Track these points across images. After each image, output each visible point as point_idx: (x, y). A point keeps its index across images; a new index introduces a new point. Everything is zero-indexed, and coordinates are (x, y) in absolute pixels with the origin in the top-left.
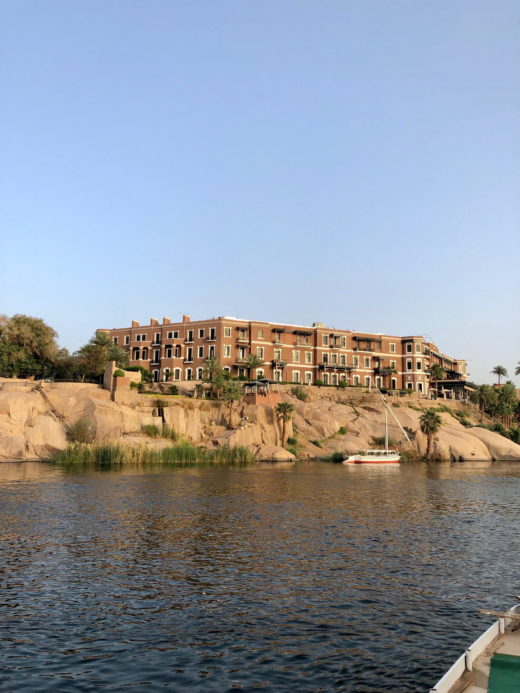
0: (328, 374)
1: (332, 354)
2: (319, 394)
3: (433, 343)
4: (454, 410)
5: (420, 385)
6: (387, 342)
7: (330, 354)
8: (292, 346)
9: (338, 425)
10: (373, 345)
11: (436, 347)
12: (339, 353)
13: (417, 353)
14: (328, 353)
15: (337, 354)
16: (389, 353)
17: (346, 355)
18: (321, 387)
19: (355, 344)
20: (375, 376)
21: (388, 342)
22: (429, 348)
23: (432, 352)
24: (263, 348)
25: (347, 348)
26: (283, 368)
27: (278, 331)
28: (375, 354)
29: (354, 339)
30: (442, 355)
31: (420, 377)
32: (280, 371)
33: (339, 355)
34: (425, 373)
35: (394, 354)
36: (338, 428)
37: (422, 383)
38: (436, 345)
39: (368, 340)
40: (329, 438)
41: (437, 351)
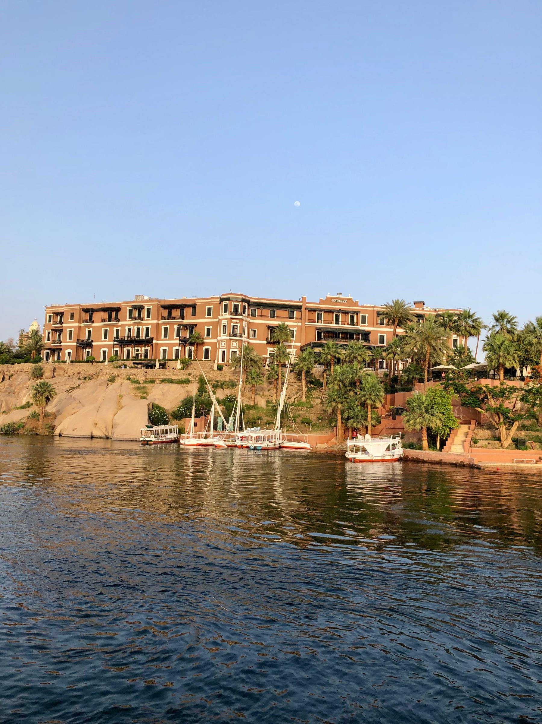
0: (130, 349)
1: (136, 327)
2: (73, 371)
3: (339, 294)
4: (217, 381)
5: (224, 352)
6: (204, 305)
7: (134, 327)
8: (101, 324)
9: (26, 399)
10: (188, 311)
11: (351, 299)
12: (143, 325)
13: (224, 314)
14: (132, 327)
15: (141, 327)
16: (205, 318)
17: (150, 327)
18: (95, 364)
19: (166, 313)
20: (185, 346)
21: (205, 305)
22: (301, 304)
23: (306, 309)
24: (73, 329)
25: (152, 320)
26: (92, 348)
27: (90, 311)
28: (186, 321)
29: (164, 307)
30: (374, 307)
31: (223, 343)
32: (90, 350)
33: (143, 327)
34: (228, 338)
35: (211, 318)
36: (24, 403)
37: (225, 350)
38: (350, 297)
39: (181, 307)
40: (5, 412)
41: (356, 304)
